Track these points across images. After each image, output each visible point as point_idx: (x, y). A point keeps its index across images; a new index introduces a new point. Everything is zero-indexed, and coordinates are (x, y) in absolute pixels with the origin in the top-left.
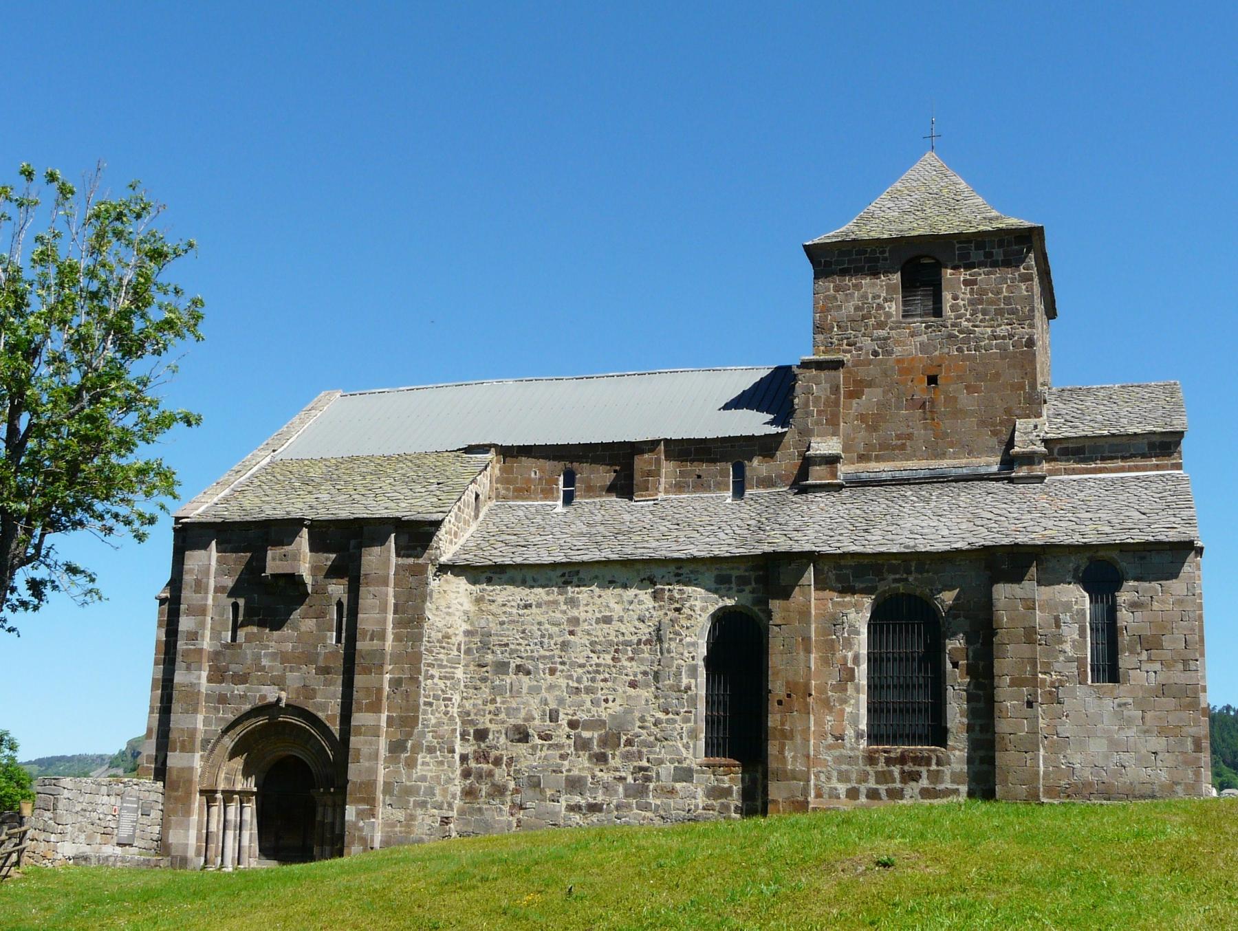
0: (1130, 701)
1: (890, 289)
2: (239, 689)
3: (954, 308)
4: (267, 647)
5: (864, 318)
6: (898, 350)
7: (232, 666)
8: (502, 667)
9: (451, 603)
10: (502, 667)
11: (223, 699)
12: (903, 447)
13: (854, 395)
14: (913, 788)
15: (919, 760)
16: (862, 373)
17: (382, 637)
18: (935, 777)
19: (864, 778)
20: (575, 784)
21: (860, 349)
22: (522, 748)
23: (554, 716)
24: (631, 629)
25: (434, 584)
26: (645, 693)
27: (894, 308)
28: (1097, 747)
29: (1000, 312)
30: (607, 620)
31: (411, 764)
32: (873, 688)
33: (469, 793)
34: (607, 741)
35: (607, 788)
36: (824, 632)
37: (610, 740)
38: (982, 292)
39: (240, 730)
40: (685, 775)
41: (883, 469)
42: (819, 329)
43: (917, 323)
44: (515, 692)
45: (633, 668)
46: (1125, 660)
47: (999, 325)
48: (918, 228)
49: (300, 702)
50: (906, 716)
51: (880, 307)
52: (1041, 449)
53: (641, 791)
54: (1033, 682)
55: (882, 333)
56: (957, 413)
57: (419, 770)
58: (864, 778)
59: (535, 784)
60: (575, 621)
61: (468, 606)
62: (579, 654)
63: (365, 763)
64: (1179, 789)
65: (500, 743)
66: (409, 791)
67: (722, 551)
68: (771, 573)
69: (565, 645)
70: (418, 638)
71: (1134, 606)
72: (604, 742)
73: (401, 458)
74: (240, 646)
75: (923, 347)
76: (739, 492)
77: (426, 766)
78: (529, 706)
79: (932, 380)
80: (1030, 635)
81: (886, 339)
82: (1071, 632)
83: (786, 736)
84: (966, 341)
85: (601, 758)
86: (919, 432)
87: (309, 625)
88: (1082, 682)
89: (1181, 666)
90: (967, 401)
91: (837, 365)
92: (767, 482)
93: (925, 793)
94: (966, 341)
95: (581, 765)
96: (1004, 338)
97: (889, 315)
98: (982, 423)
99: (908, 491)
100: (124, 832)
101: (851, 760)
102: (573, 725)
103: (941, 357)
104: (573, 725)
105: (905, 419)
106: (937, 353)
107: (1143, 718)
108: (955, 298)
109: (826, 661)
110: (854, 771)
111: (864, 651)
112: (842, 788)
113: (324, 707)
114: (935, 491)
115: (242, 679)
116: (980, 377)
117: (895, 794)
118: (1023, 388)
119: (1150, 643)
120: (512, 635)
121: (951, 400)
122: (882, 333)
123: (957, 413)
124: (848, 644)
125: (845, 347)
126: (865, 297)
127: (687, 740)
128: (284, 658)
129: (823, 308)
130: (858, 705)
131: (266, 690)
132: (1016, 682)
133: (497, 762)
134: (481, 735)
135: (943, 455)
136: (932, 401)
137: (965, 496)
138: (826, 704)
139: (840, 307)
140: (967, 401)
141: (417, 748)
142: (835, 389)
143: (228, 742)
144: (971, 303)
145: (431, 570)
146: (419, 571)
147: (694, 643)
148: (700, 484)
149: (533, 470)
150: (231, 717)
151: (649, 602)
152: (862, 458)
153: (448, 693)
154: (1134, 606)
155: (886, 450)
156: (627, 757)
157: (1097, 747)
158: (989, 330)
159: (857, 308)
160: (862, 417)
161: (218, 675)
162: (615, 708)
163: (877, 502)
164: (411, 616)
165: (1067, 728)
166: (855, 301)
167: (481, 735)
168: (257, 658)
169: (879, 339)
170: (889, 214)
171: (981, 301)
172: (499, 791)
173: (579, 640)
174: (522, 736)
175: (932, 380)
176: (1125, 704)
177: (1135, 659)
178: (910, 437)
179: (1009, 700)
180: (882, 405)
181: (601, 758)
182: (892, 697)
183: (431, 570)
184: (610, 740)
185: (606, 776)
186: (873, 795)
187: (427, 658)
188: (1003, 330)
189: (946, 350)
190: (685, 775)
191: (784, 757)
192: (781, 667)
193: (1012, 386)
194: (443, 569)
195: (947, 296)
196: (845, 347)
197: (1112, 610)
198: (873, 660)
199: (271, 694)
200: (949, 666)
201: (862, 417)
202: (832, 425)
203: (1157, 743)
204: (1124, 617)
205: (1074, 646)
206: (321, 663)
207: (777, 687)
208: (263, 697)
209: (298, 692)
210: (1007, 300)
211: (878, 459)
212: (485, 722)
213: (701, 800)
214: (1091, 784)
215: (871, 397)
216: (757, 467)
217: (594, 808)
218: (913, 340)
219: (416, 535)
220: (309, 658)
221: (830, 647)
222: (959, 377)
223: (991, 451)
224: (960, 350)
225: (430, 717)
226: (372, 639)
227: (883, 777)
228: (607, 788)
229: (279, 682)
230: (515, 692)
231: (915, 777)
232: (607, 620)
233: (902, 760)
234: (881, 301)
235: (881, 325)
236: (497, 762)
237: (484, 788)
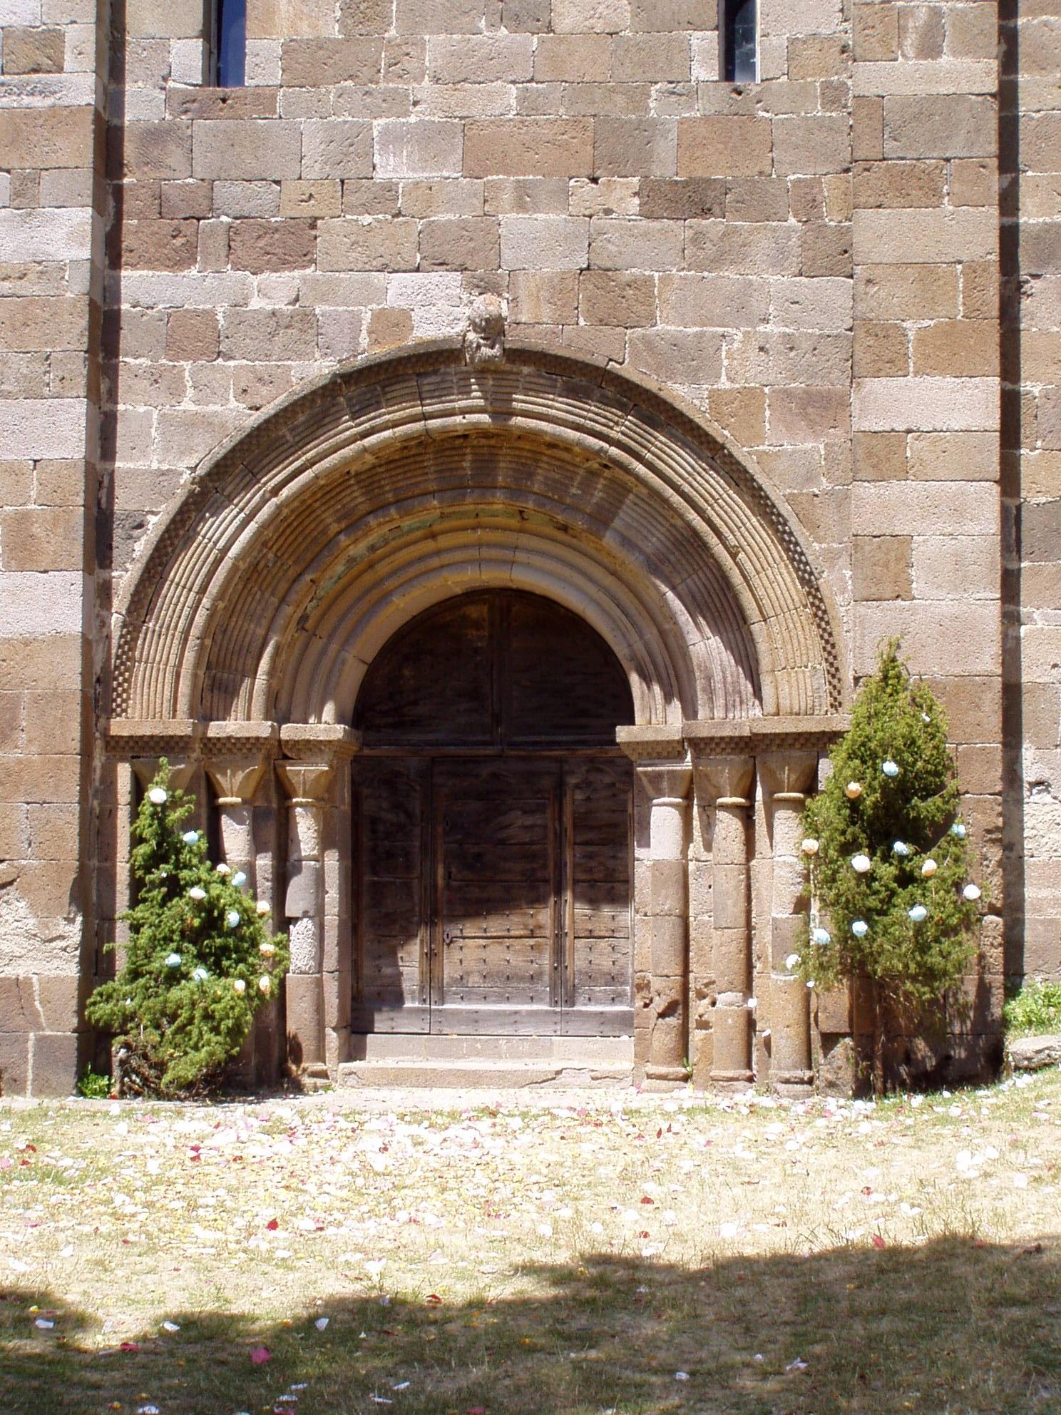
2: (272, 291)
4: (400, 103)
7: (231, 195)
49: (580, 338)
74: (264, 101)
113: (697, 359)
115: (292, 244)
128: (481, 151)
131: (398, 289)
150: (238, 415)
168: (355, 145)
199: (439, 310)
206: (667, 164)
208: (401, 320)
209: (559, 290)
220: (612, 147)
226: (930, 49)
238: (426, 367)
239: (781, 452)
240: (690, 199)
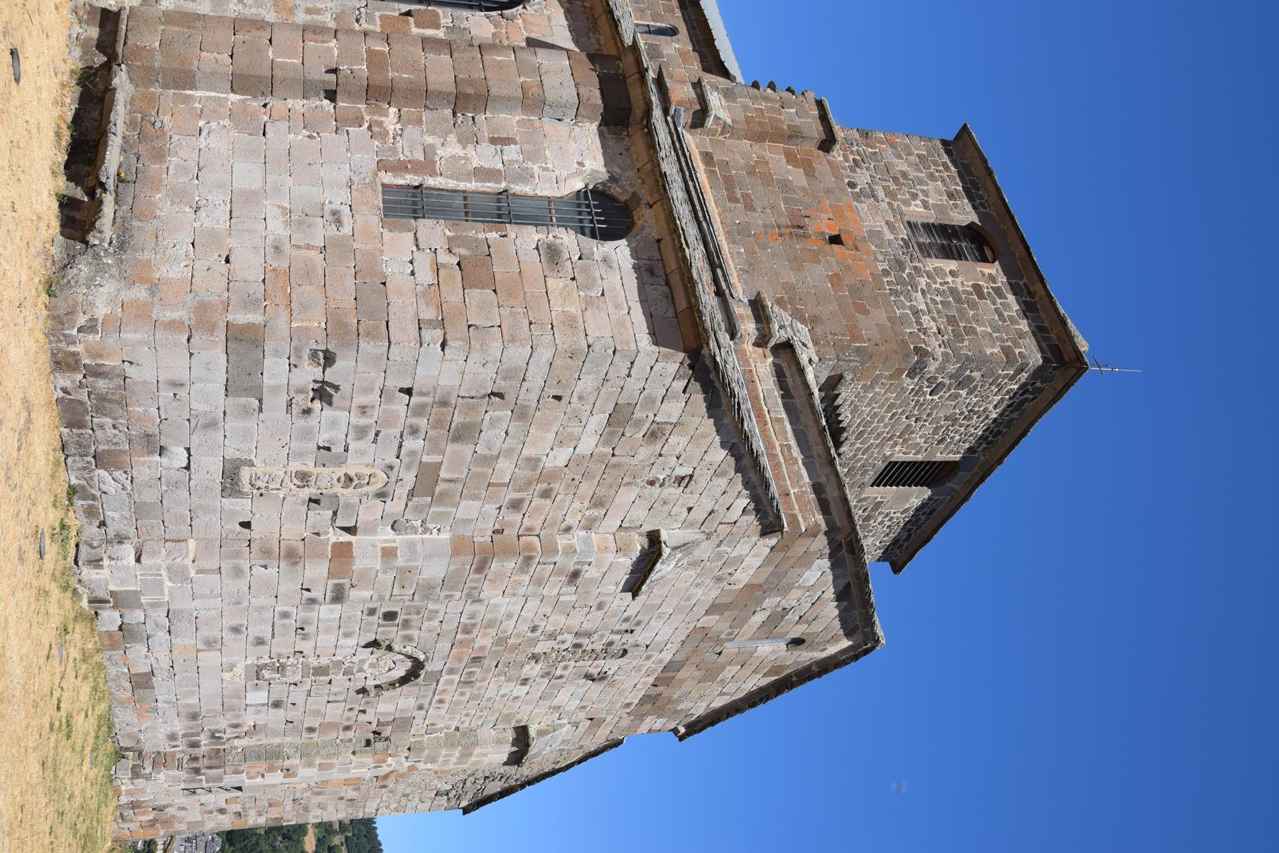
0: (346, 230)
1: (940, 209)
3: (938, 271)
5: (895, 179)
6: (863, 207)
12: (732, 198)
13: (791, 158)
21: (854, 171)
27: (916, 211)
28: (248, 175)
29: (951, 320)
38: (973, 306)
46: (434, 231)
47: (934, 319)
51: (914, 196)
55: (881, 194)
64: (140, 293)
79: (835, 240)
81: (874, 196)
82: (484, 156)
84: (900, 281)
86: (758, 219)
88: (382, 166)
89: (429, 314)
94: (900, 281)
96: (919, 323)
97: (906, 203)
98: (790, 288)
103: (868, 252)
106: (873, 248)
107: (308, 247)
108: (952, 273)
116: (855, 291)
118: (855, 338)
119: (475, 270)
121: (815, 257)
122: (881, 194)
125: (851, 157)
126: (921, 182)
135: (732, 241)
136: (806, 236)
139: (900, 157)
144: (953, 291)
152: (708, 158)
154: (552, 254)
157: (248, 175)
158: (923, 307)
159: (904, 175)
165: (282, 137)
169: (873, 191)
171: (958, 300)
175: (835, 240)
176: (338, 222)
177: (441, 244)
178: (750, 207)
180: (785, 185)
189: (880, 257)
193: (854, 327)
196: (851, 157)
200: (405, 8)
203: (249, 267)
204: (527, 238)
205: (455, 158)
210: (970, 331)
211: (711, 174)
214: (160, 156)
222: (848, 268)
224: (886, 273)
234: (921, 197)
235: (889, 193)
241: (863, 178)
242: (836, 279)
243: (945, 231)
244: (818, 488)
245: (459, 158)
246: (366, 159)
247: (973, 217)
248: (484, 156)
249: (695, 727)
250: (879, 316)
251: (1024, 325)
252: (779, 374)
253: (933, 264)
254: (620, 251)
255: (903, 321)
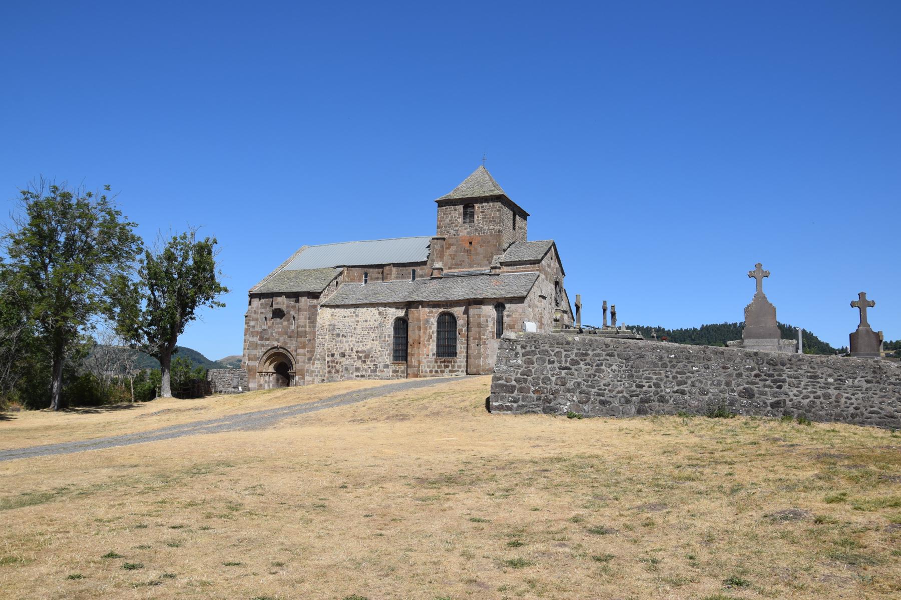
1: (460, 214)
2: (267, 342)
6: (461, 234)
8: (338, 335)
9: (325, 316)
10: (338, 335)
11: (263, 345)
13: (448, 248)
14: (447, 370)
15: (448, 362)
16: (450, 241)
17: (305, 327)
18: (453, 366)
19: (434, 367)
20: (357, 369)
22: (344, 359)
23: (352, 350)
24: (372, 323)
25: (319, 311)
26: (376, 343)
27: (460, 220)
30: (366, 321)
31: (313, 364)
32: (438, 339)
33: (329, 372)
34: (365, 357)
35: (366, 370)
36: (424, 324)
37: (367, 356)
39: (268, 354)
40: (386, 366)
41: (455, 271)
42: (438, 227)
43: (467, 226)
44: (342, 342)
45: (373, 335)
48: (469, 194)
50: (446, 350)
52: (499, 265)
53: (375, 371)
54: (480, 339)
56: (477, 254)
57: (316, 366)
58: (434, 367)
59: (347, 369)
60: (358, 321)
61: (329, 317)
62: (359, 331)
63: (301, 364)
65: (338, 357)
66: (313, 372)
67: (396, 301)
68: (409, 305)
69: (355, 329)
70: (315, 327)
71: (508, 316)
72: (365, 357)
73: (317, 270)
75: (468, 233)
76: (414, 278)
77: (318, 365)
78: (346, 347)
79: (471, 243)
80: (479, 325)
82: (490, 324)
83: (413, 355)
85: (365, 362)
86: (466, 260)
87: (285, 323)
90: (480, 250)
91: (444, 239)
92: (421, 276)
93: (451, 371)
95: (359, 364)
99: (459, 279)
100: (235, 384)
101: (431, 362)
102: (357, 352)
104: (357, 352)
105: (462, 256)
109: (425, 333)
110: (431, 365)
111: (435, 330)
112: (428, 370)
114: (465, 280)
115: (268, 339)
116: (484, 242)
117: (442, 372)
120: (341, 326)
121: (475, 249)
123: (477, 254)
124: (431, 328)
127: (386, 357)
128: (279, 333)
129: (441, 220)
130: (433, 347)
132: (475, 339)
133: (337, 363)
134: (333, 355)
137: (474, 281)
138: (424, 345)
140: (480, 250)
141: (315, 359)
142: (442, 247)
143: (265, 358)
145: (319, 307)
146: (315, 307)
147: (389, 329)
148: (403, 276)
149: (356, 273)
151: (378, 316)
152: (450, 268)
153: (324, 343)
154: (508, 316)
155: (457, 265)
156: (371, 361)
160: (450, 255)
161: (261, 339)
162: (368, 347)
163: (449, 283)
164: (313, 320)
166: (449, 218)
167: (333, 355)
170: (464, 189)
172: (337, 371)
173: (359, 327)
174: (343, 355)
175: (471, 243)
179: (472, 345)
180: (456, 251)
181: (365, 362)
182: (442, 342)
183: (319, 307)
184: (367, 356)
185: (366, 367)
186: (437, 372)
187: (318, 333)
188: (491, 227)
190: (386, 366)
191: (413, 361)
192: (412, 336)
194: (322, 306)
195: (476, 216)
197: (502, 317)
198: (438, 332)
199: (276, 344)
201: (450, 255)
202: (441, 257)
204: (505, 319)
207: (410, 340)
212: (333, 351)
213: (391, 374)
215: (453, 248)
216: (419, 270)
217: (362, 376)
218: (464, 231)
219: (315, 295)
220: (286, 333)
221: (426, 329)
223: (486, 266)
225: (318, 350)
227: (439, 367)
228: (366, 370)
229: (278, 340)
230: (342, 342)
231: (447, 366)
232: (366, 321)
233: (444, 362)
235: (456, 226)
236: (337, 363)
237: (333, 371)
238: (276, 347)
239: (294, 353)
240: (290, 337)
241: (452, 231)
242: (481, 246)
243: (465, 214)
244: (531, 264)
245: (492, 327)
246: (492, 341)
247: (462, 206)
248: (490, 324)
249: (563, 274)
250: (490, 238)
251: (491, 204)
252: (506, 266)
253: (476, 221)
254: (507, 306)
255: (491, 233)
